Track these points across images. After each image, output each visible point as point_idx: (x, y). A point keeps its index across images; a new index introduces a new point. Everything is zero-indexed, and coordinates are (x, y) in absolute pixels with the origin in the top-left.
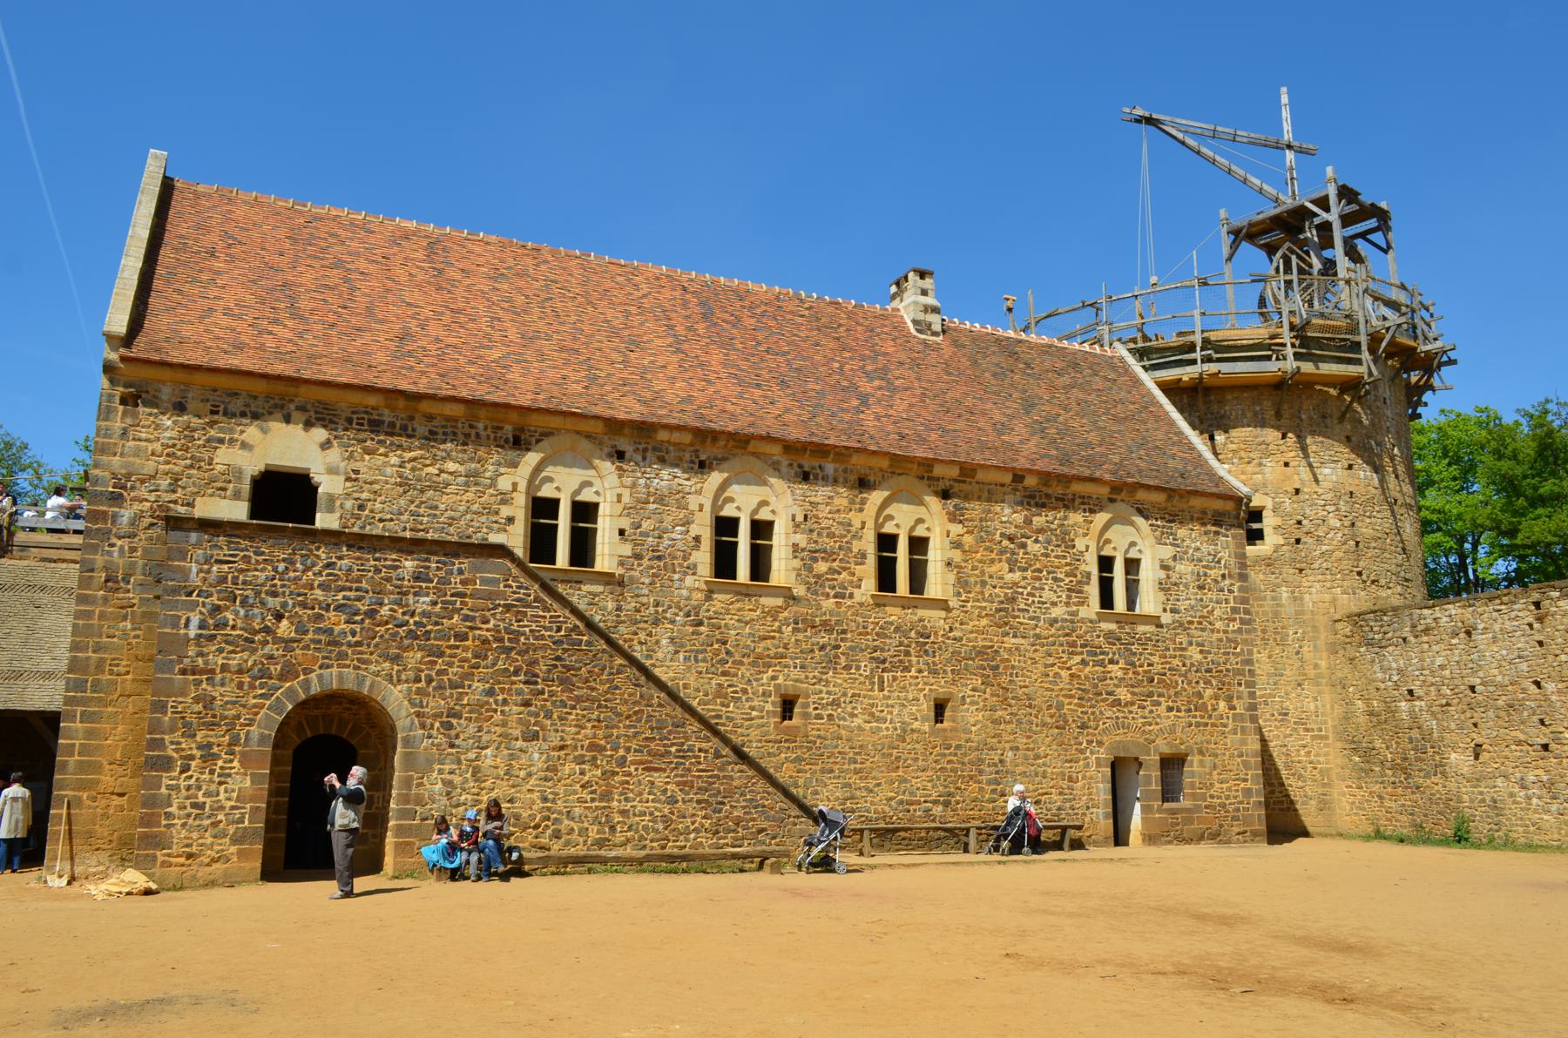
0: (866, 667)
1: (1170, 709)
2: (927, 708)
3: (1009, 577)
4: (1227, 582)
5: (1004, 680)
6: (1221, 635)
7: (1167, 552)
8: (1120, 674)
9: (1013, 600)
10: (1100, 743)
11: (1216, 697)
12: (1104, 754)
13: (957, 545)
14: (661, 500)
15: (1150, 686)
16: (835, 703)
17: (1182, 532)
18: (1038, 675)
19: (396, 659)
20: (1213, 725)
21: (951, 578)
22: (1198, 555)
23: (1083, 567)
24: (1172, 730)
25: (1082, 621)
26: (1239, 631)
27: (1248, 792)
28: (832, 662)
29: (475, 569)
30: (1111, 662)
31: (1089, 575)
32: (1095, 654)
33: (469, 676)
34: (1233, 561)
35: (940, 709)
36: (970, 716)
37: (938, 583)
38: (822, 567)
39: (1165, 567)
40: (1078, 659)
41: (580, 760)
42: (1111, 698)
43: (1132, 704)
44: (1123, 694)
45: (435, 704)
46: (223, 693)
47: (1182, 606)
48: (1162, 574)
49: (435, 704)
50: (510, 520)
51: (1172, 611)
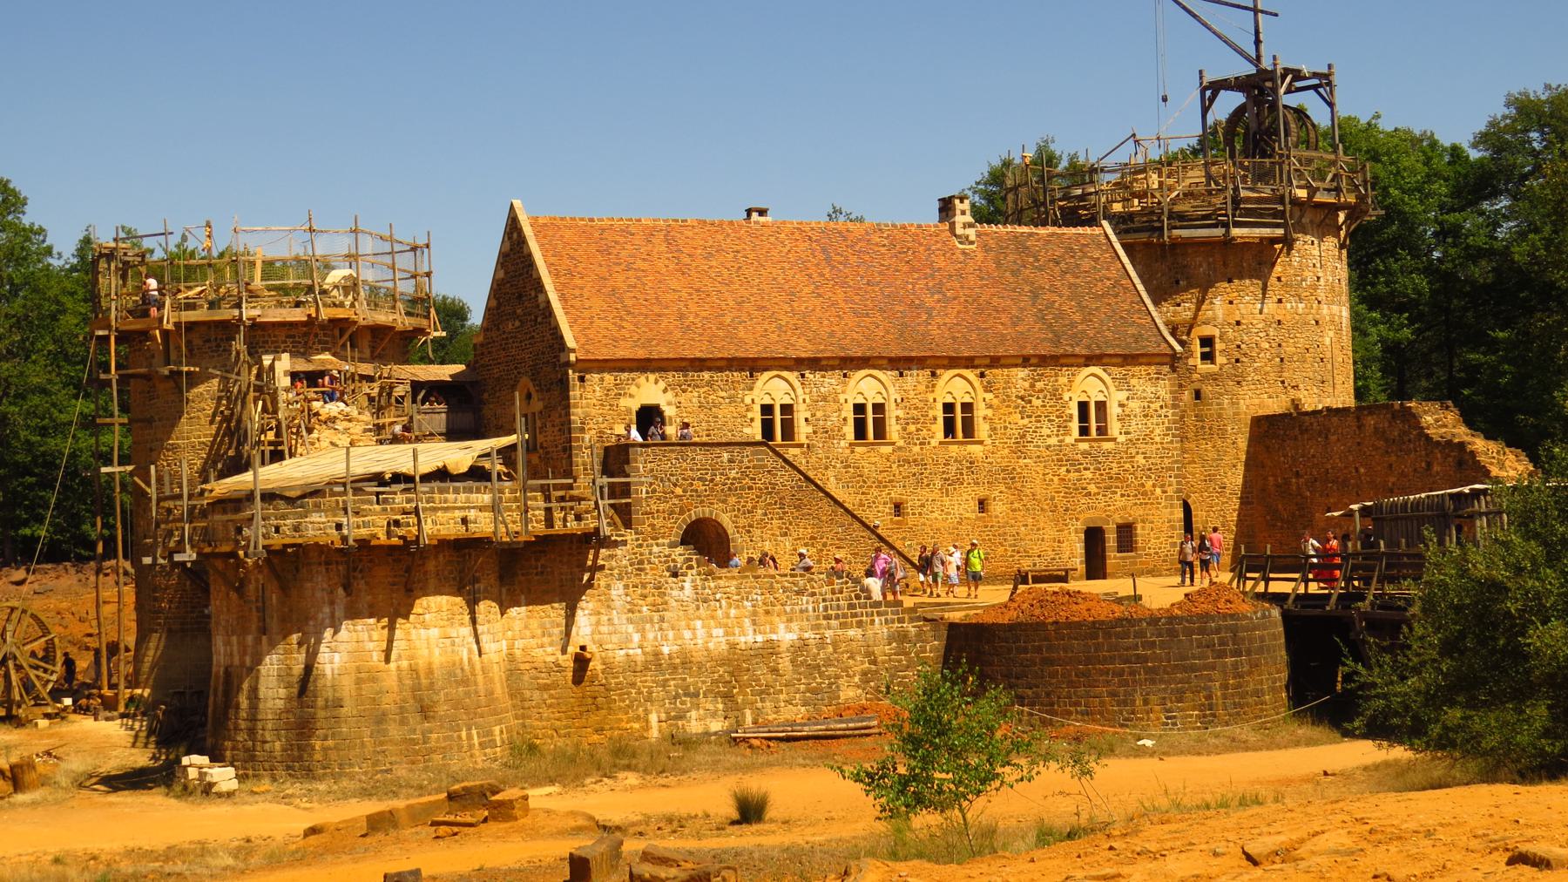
0: (938, 483)
2: (974, 505)
3: (1021, 422)
5: (1019, 485)
9: (1023, 436)
12: (1081, 526)
13: (990, 406)
14: (825, 399)
15: (1111, 482)
16: (923, 506)
17: (1134, 381)
18: (1038, 478)
19: (724, 502)
21: (987, 427)
24: (1124, 508)
28: (919, 482)
29: (753, 454)
31: (1071, 416)
33: (755, 507)
35: (982, 505)
36: (998, 508)
37: (982, 430)
38: (912, 428)
39: (1121, 405)
41: (806, 545)
44: (1092, 488)
45: (742, 521)
46: (658, 522)
48: (1119, 410)
49: (742, 521)
50: (752, 420)
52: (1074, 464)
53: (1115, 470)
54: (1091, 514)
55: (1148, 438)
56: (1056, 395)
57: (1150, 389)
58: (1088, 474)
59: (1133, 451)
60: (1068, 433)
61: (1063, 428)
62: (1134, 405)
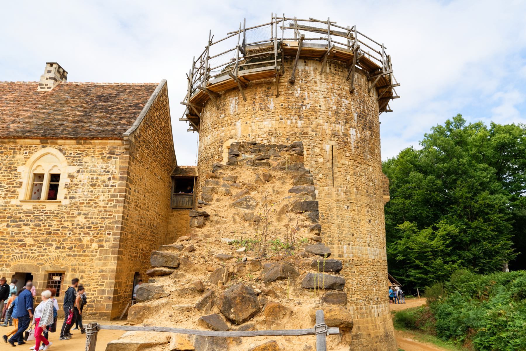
1: (58, 248)
4: (112, 181)
6: (102, 209)
7: (73, 170)
8: (29, 231)
10: (8, 265)
11: (92, 241)
17: (86, 159)
20: (85, 256)
22: (95, 169)
23: (18, 180)
25: (12, 206)
26: (115, 206)
27: (103, 292)
30: (26, 225)
31: (21, 184)
32: (16, 221)
34: (117, 171)
39: (71, 177)
40: (5, 224)
42: (20, 243)
43: (33, 245)
44: (29, 241)
47: (77, 195)
48: (68, 181)
51: (70, 198)
52: (15, 221)
53: (55, 227)
54: (22, 262)
55: (91, 203)
56: (12, 168)
57: (99, 165)
58: (28, 229)
59: (76, 213)
60: (14, 195)
61: (12, 192)
62: (84, 178)
